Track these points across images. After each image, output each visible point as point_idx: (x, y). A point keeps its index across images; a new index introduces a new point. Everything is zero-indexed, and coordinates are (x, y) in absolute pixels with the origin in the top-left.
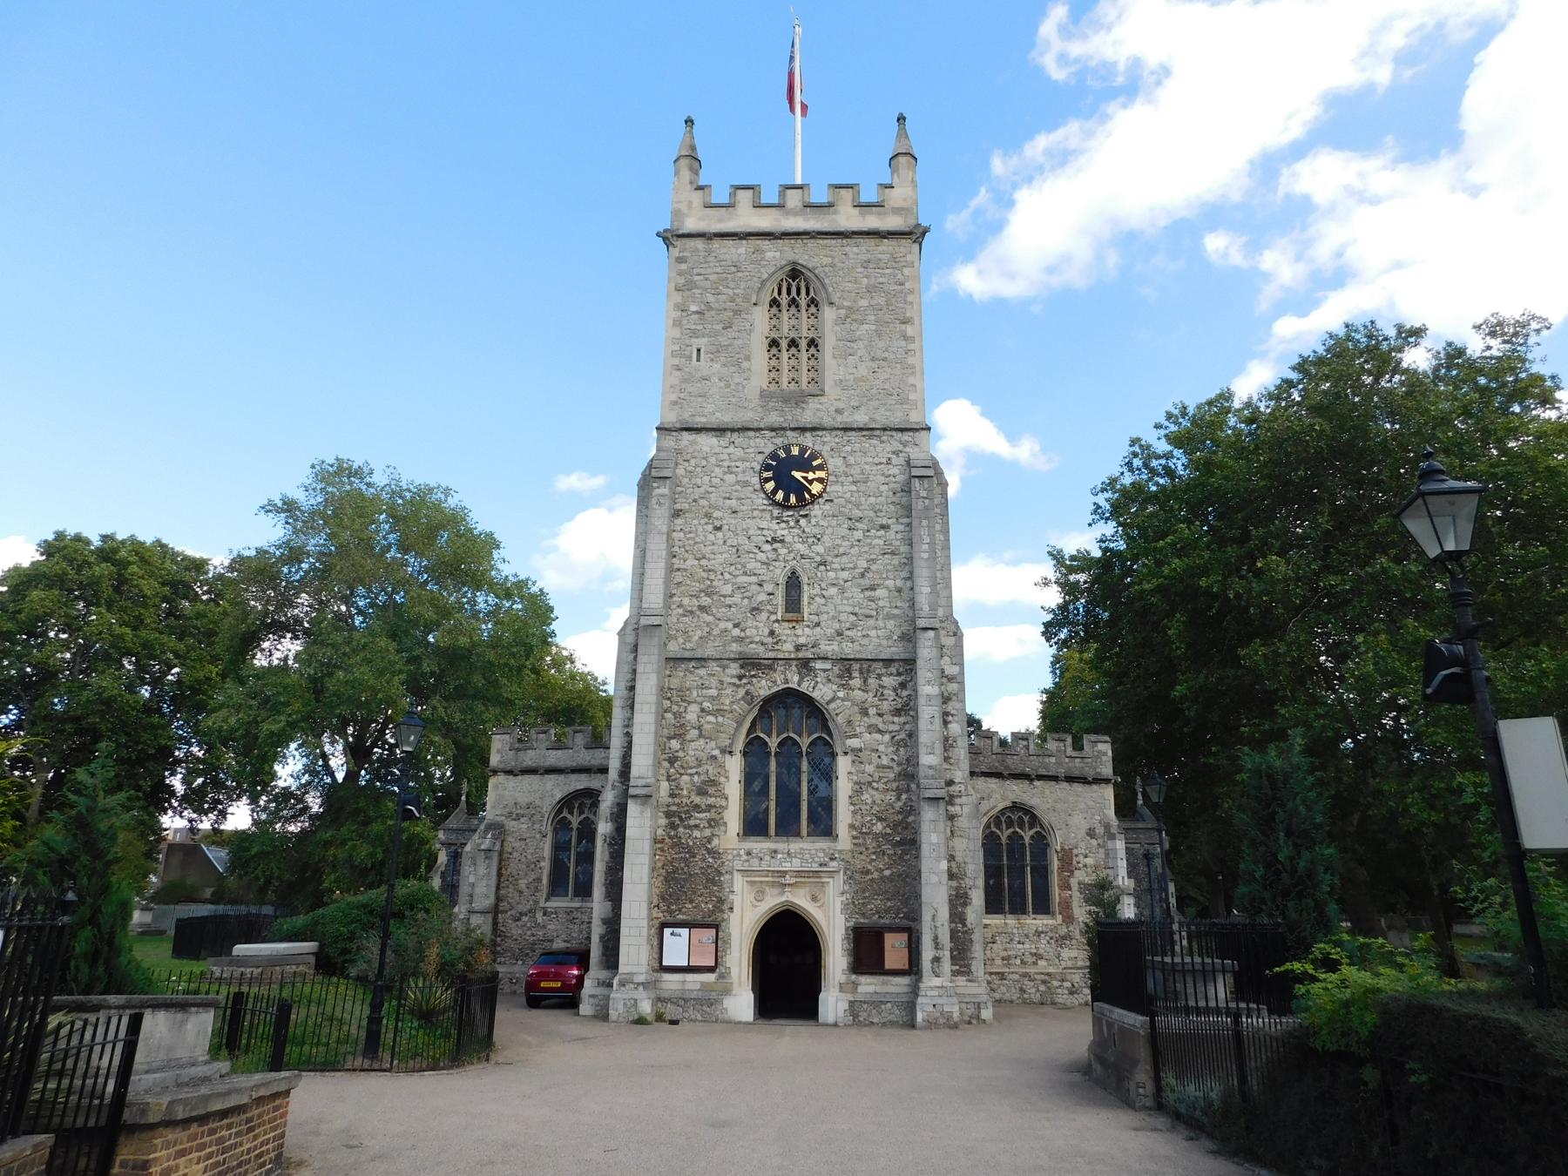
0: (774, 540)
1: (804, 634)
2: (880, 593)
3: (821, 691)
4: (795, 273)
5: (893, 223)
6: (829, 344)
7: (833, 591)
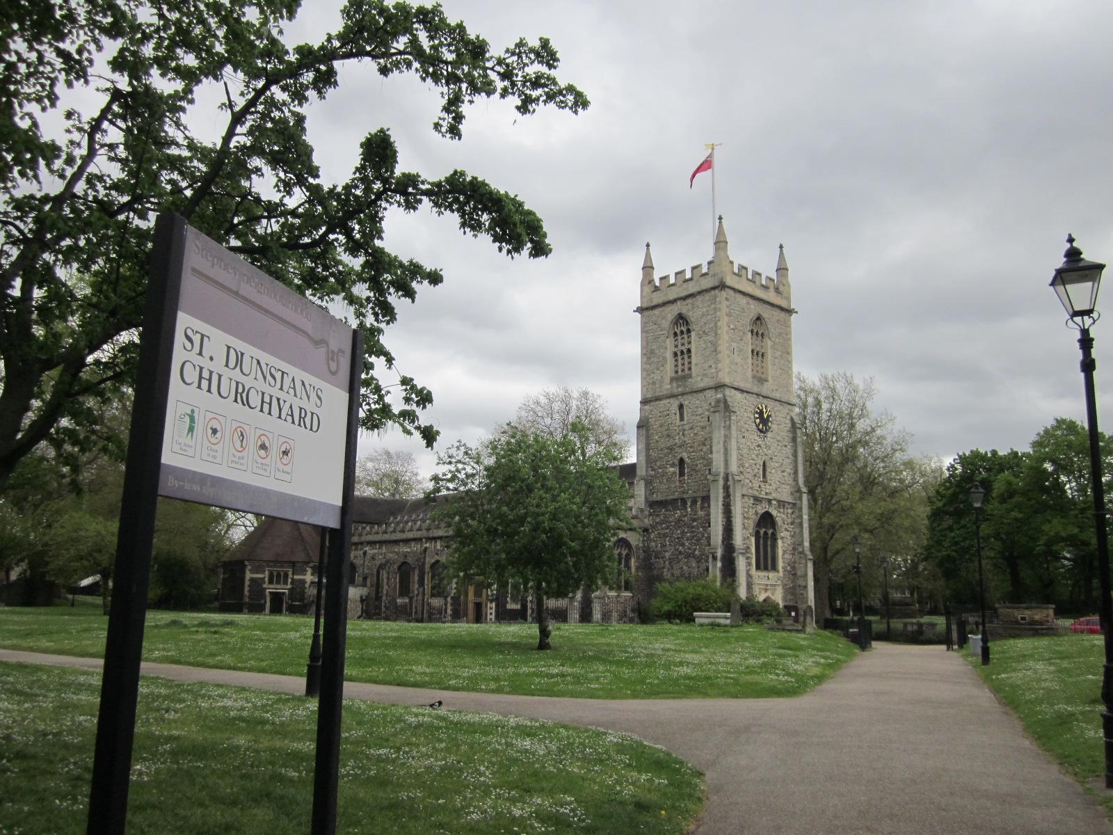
0: (759, 446)
1: (768, 488)
2: (785, 474)
3: (774, 513)
4: (758, 318)
5: (783, 304)
6: (769, 356)
7: (773, 471)
